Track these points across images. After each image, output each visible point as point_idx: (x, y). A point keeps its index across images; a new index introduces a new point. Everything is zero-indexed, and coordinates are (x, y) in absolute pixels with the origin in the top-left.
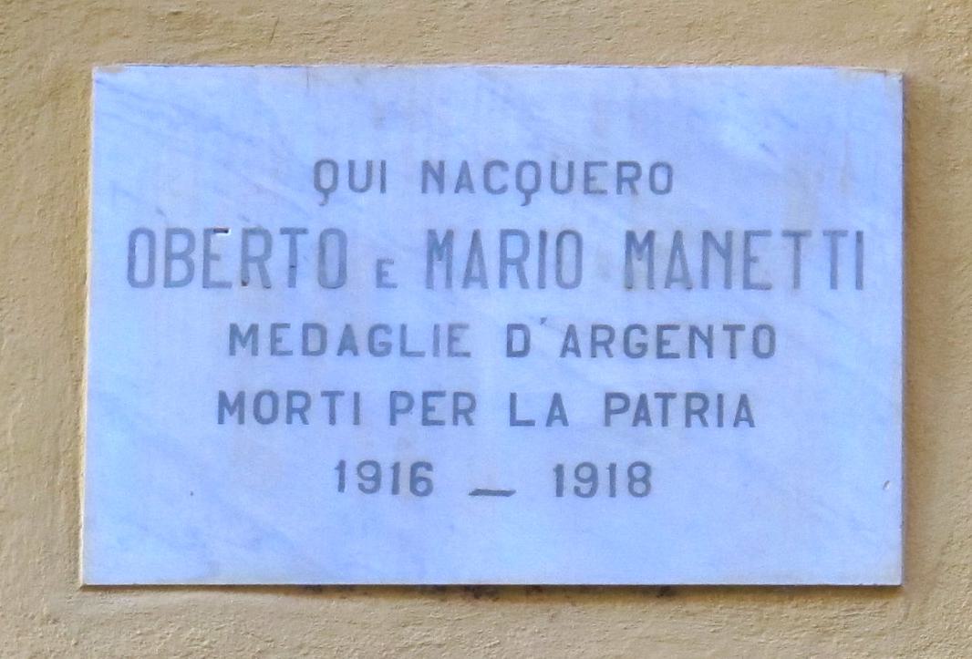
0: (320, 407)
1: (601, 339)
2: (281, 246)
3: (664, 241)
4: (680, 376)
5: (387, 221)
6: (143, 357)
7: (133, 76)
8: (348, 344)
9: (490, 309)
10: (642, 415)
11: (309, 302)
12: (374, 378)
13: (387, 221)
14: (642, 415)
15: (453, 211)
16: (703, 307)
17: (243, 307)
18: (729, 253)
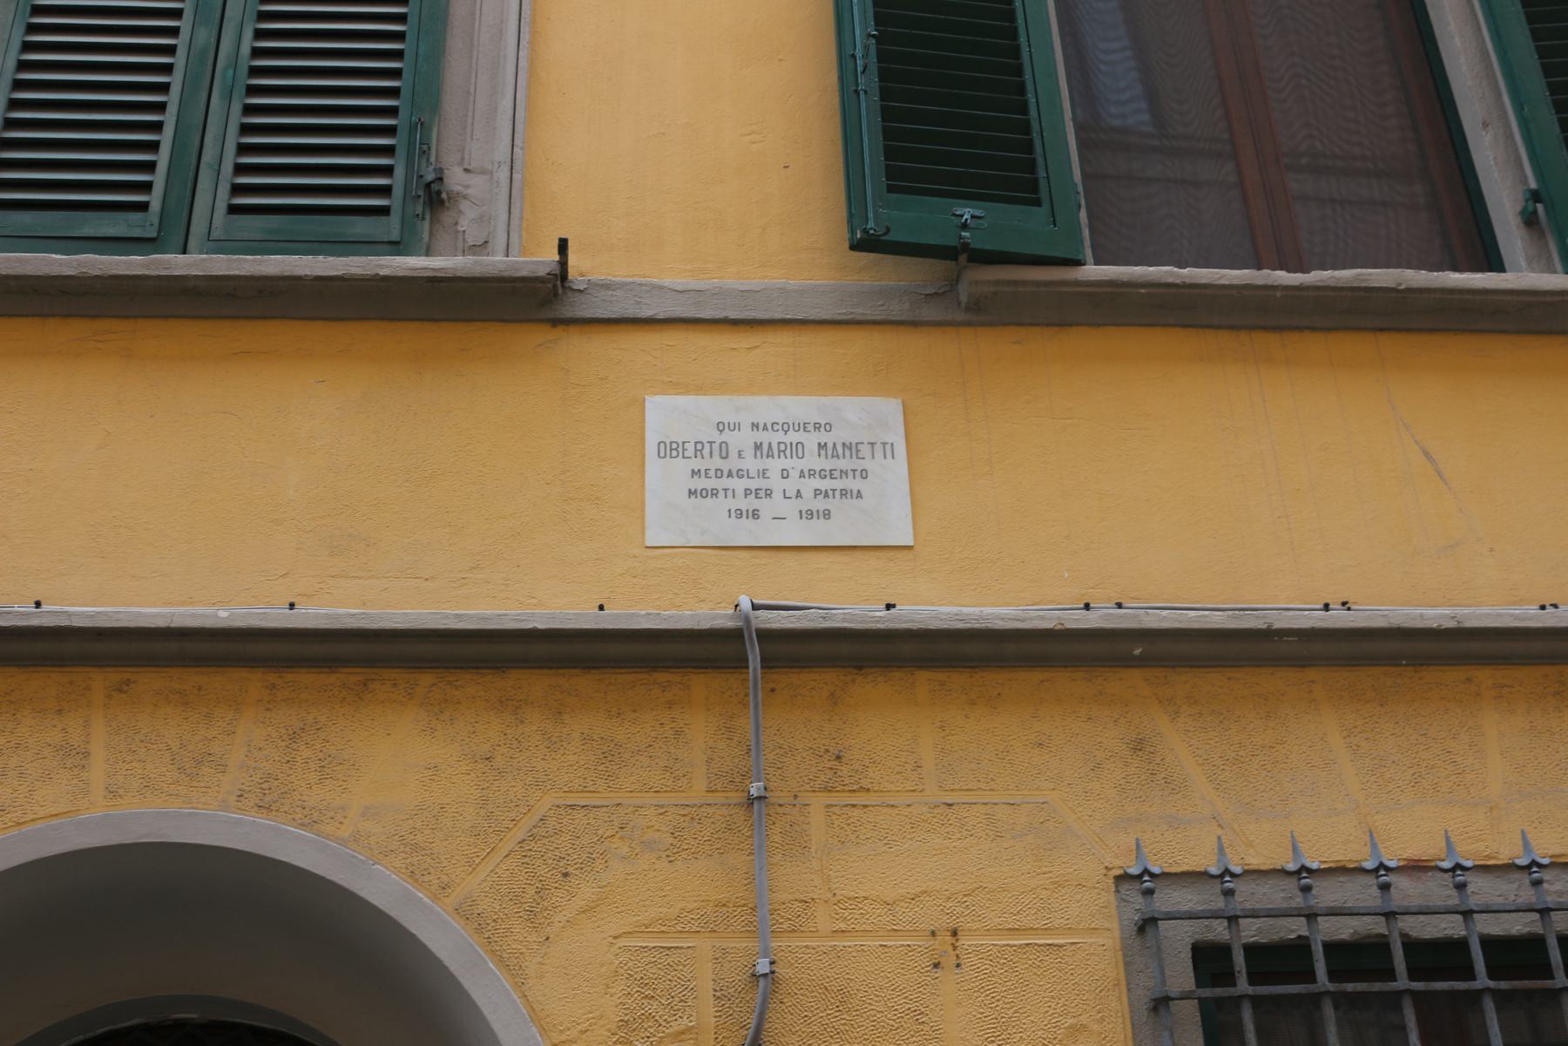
0: (722, 493)
1: (812, 473)
2: (707, 446)
3: (830, 446)
4: (838, 484)
5: (742, 440)
6: (664, 482)
7: (658, 398)
8: (730, 475)
9: (775, 465)
10: (826, 495)
11: (717, 462)
12: (739, 485)
13: (742, 440)
14: (826, 495)
15: (764, 437)
16: (843, 464)
17: (697, 464)
18: (851, 448)
